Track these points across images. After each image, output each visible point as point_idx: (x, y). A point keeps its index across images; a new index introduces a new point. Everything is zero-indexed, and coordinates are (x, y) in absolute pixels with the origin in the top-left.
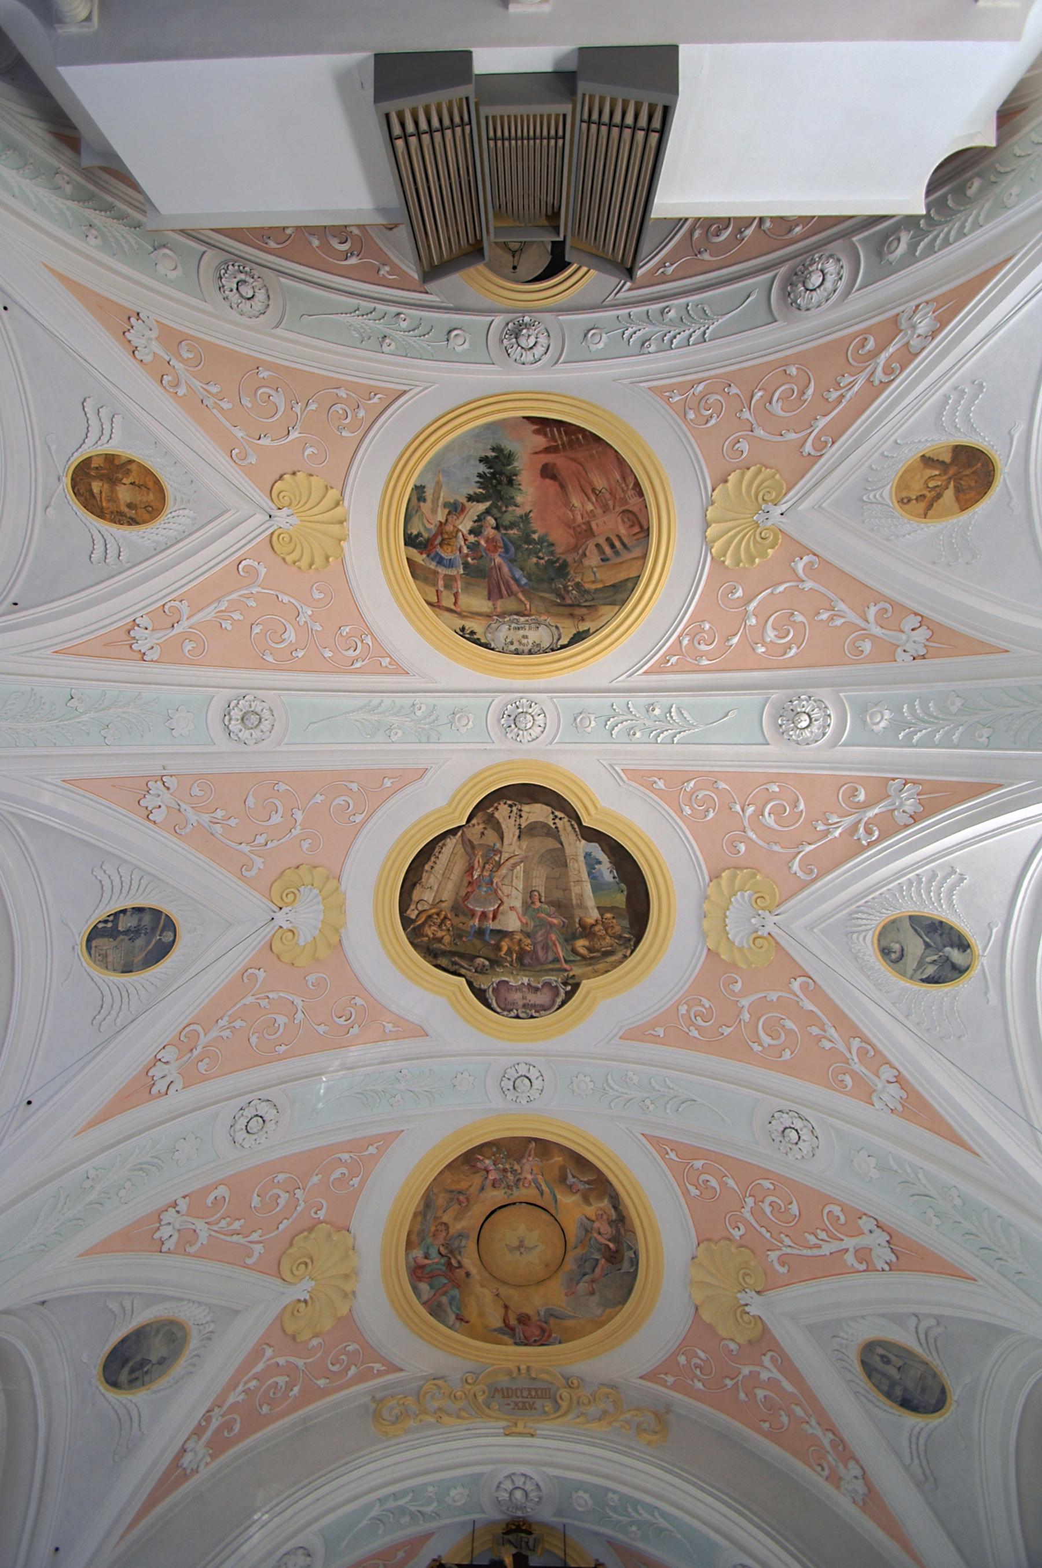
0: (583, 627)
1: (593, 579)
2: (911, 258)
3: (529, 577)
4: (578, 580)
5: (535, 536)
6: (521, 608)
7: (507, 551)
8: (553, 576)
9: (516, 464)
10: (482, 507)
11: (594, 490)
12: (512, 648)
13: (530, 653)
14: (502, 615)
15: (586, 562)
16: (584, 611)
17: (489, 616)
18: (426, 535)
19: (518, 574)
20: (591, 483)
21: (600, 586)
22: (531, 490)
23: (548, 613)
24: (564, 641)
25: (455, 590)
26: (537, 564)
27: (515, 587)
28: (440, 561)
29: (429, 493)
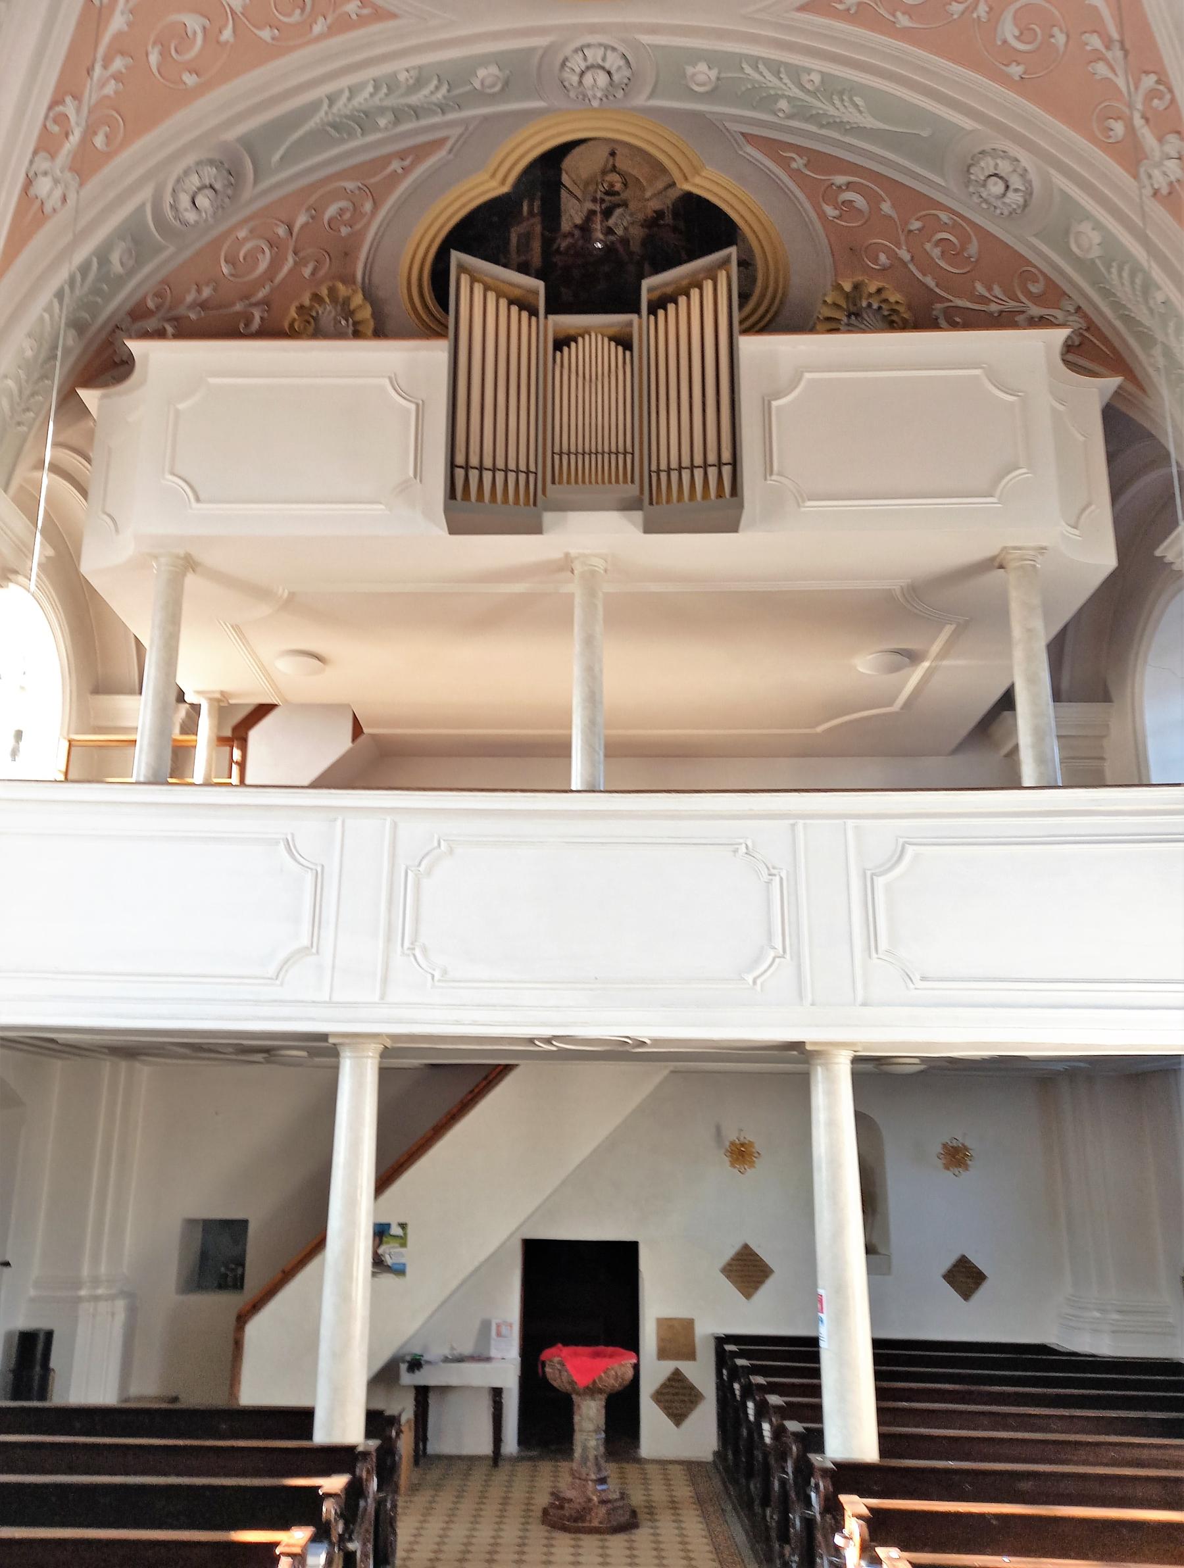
2: (102, 254)
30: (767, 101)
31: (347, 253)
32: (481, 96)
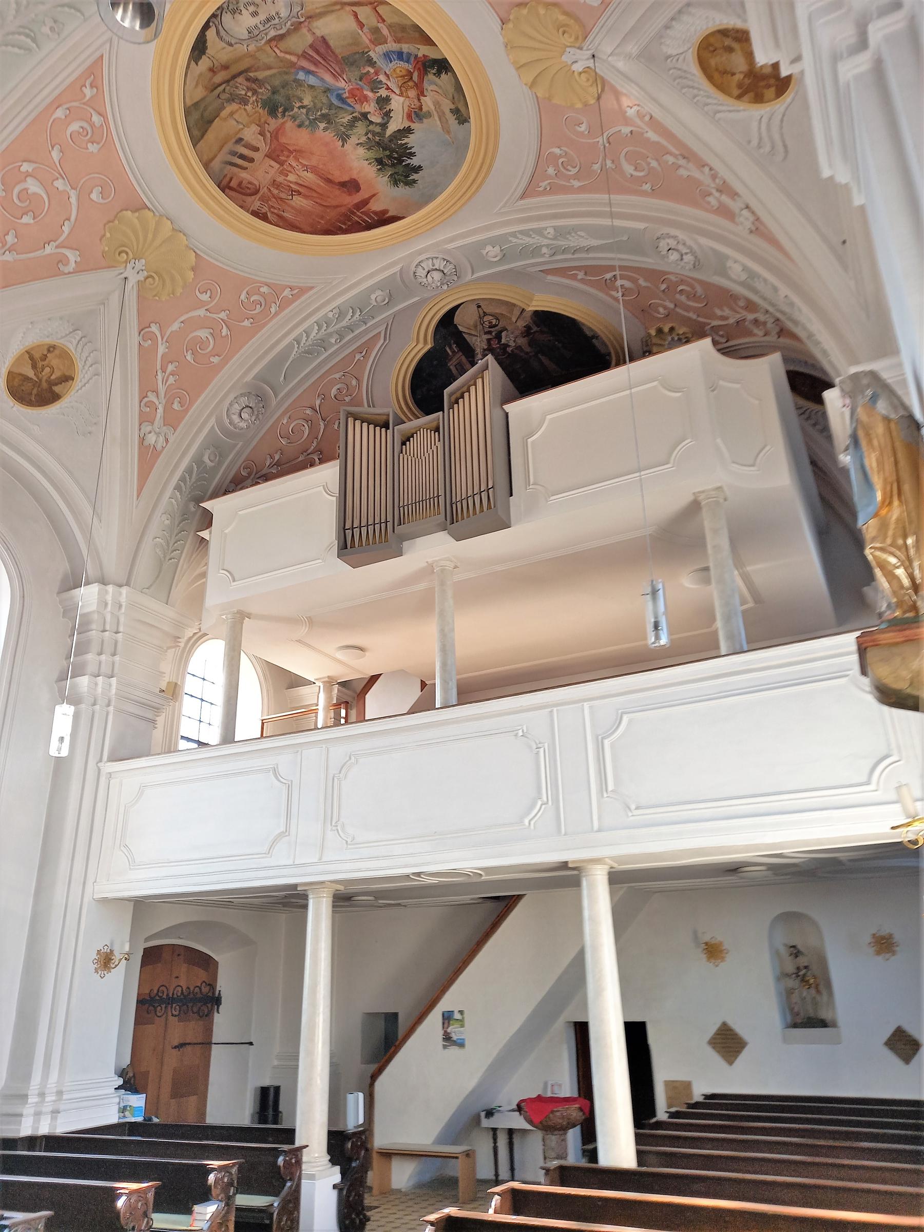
5: (322, 125)
7: (340, 97)
8: (276, 97)
9: (386, 179)
19: (312, 80)
25: (365, 29)
26: (301, 100)
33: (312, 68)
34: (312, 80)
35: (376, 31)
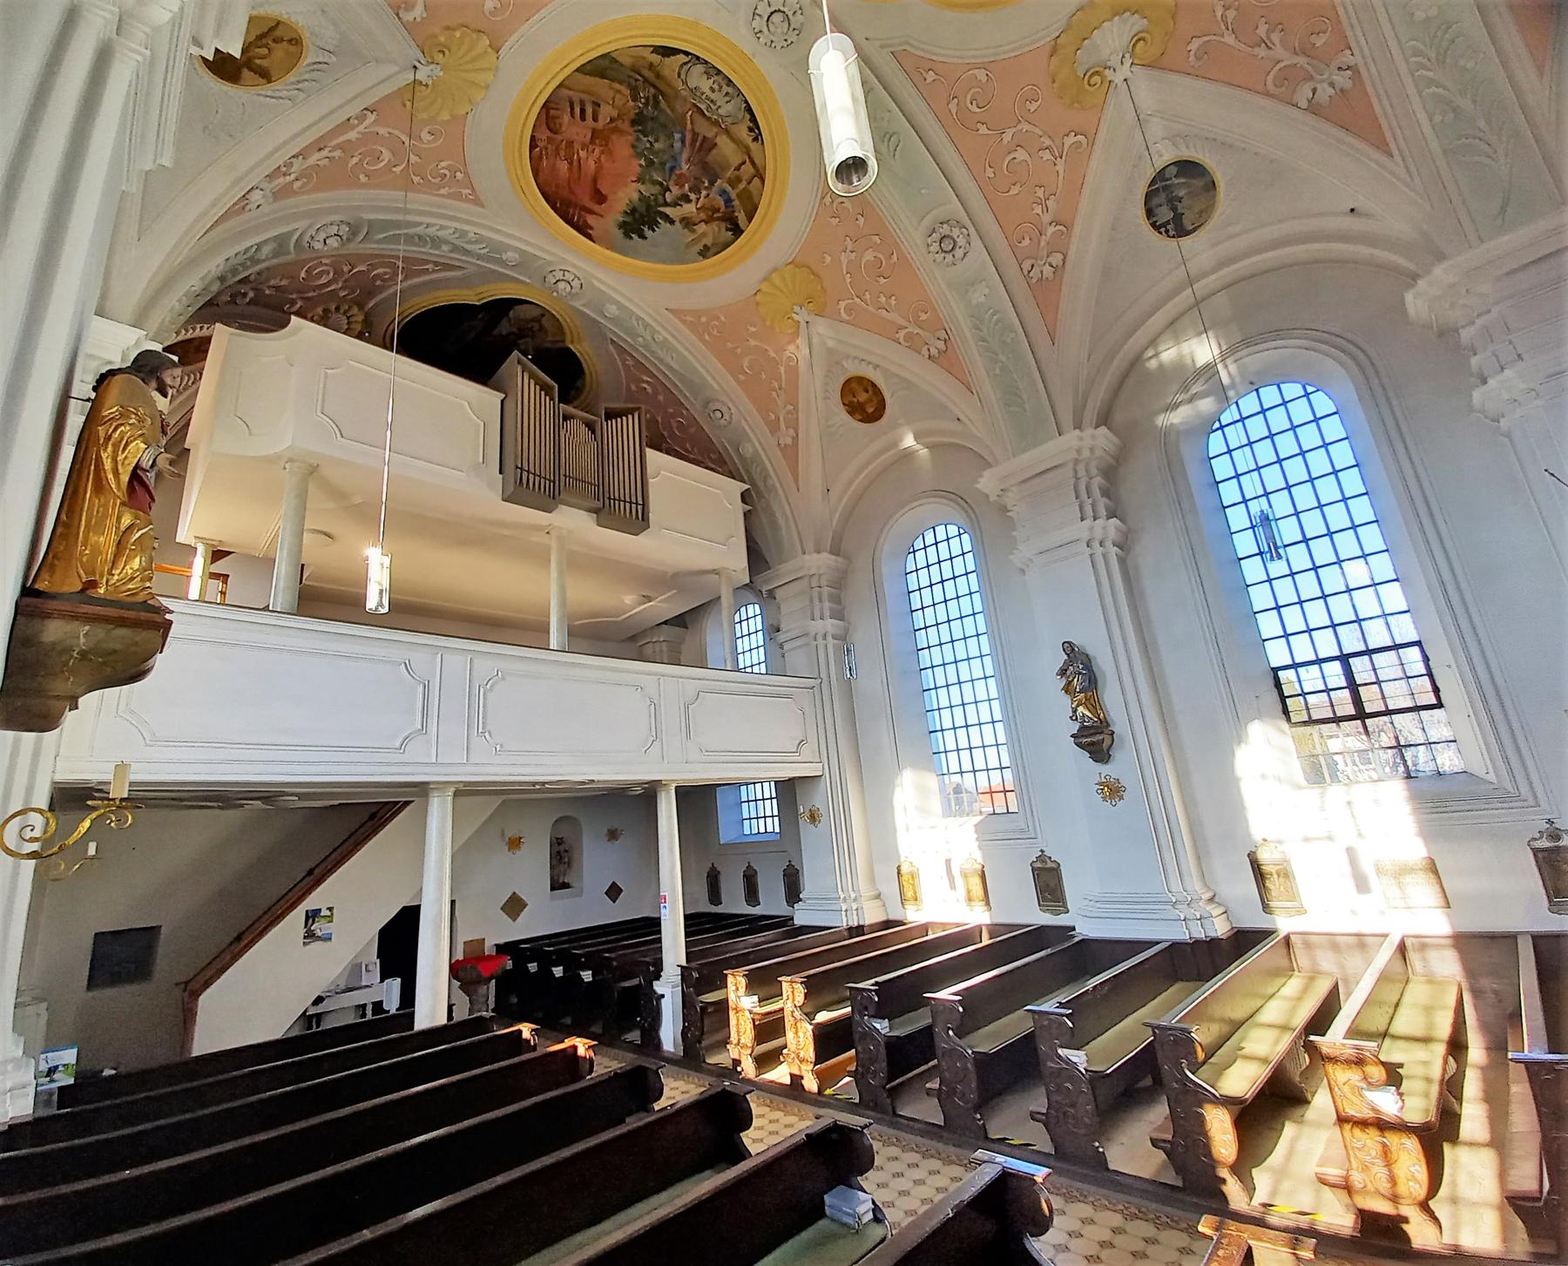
0: (656, 58)
1: (618, 96)
3: (670, 136)
4: (631, 103)
5: (643, 162)
6: (697, 117)
10: (668, 210)
11: (571, 164)
12: (730, 90)
13: (719, 72)
14: (716, 123)
15: (615, 114)
16: (646, 73)
17: (727, 131)
18: (723, 225)
19: (678, 145)
20: (570, 169)
21: (616, 86)
22: (621, 194)
23: (677, 92)
24: (682, 58)
27: (689, 137)
28: (728, 201)
29: (700, 247)
30: (635, 335)
31: (370, 294)
32: (503, 263)
33: (688, 142)
34: (678, 145)
35: (739, 180)
